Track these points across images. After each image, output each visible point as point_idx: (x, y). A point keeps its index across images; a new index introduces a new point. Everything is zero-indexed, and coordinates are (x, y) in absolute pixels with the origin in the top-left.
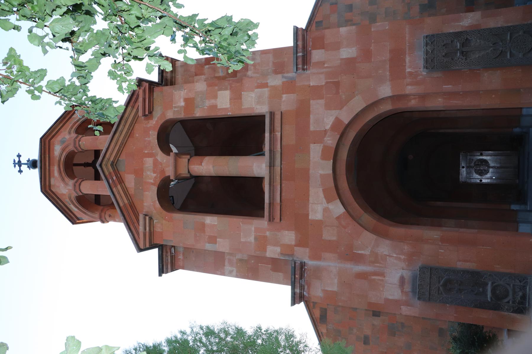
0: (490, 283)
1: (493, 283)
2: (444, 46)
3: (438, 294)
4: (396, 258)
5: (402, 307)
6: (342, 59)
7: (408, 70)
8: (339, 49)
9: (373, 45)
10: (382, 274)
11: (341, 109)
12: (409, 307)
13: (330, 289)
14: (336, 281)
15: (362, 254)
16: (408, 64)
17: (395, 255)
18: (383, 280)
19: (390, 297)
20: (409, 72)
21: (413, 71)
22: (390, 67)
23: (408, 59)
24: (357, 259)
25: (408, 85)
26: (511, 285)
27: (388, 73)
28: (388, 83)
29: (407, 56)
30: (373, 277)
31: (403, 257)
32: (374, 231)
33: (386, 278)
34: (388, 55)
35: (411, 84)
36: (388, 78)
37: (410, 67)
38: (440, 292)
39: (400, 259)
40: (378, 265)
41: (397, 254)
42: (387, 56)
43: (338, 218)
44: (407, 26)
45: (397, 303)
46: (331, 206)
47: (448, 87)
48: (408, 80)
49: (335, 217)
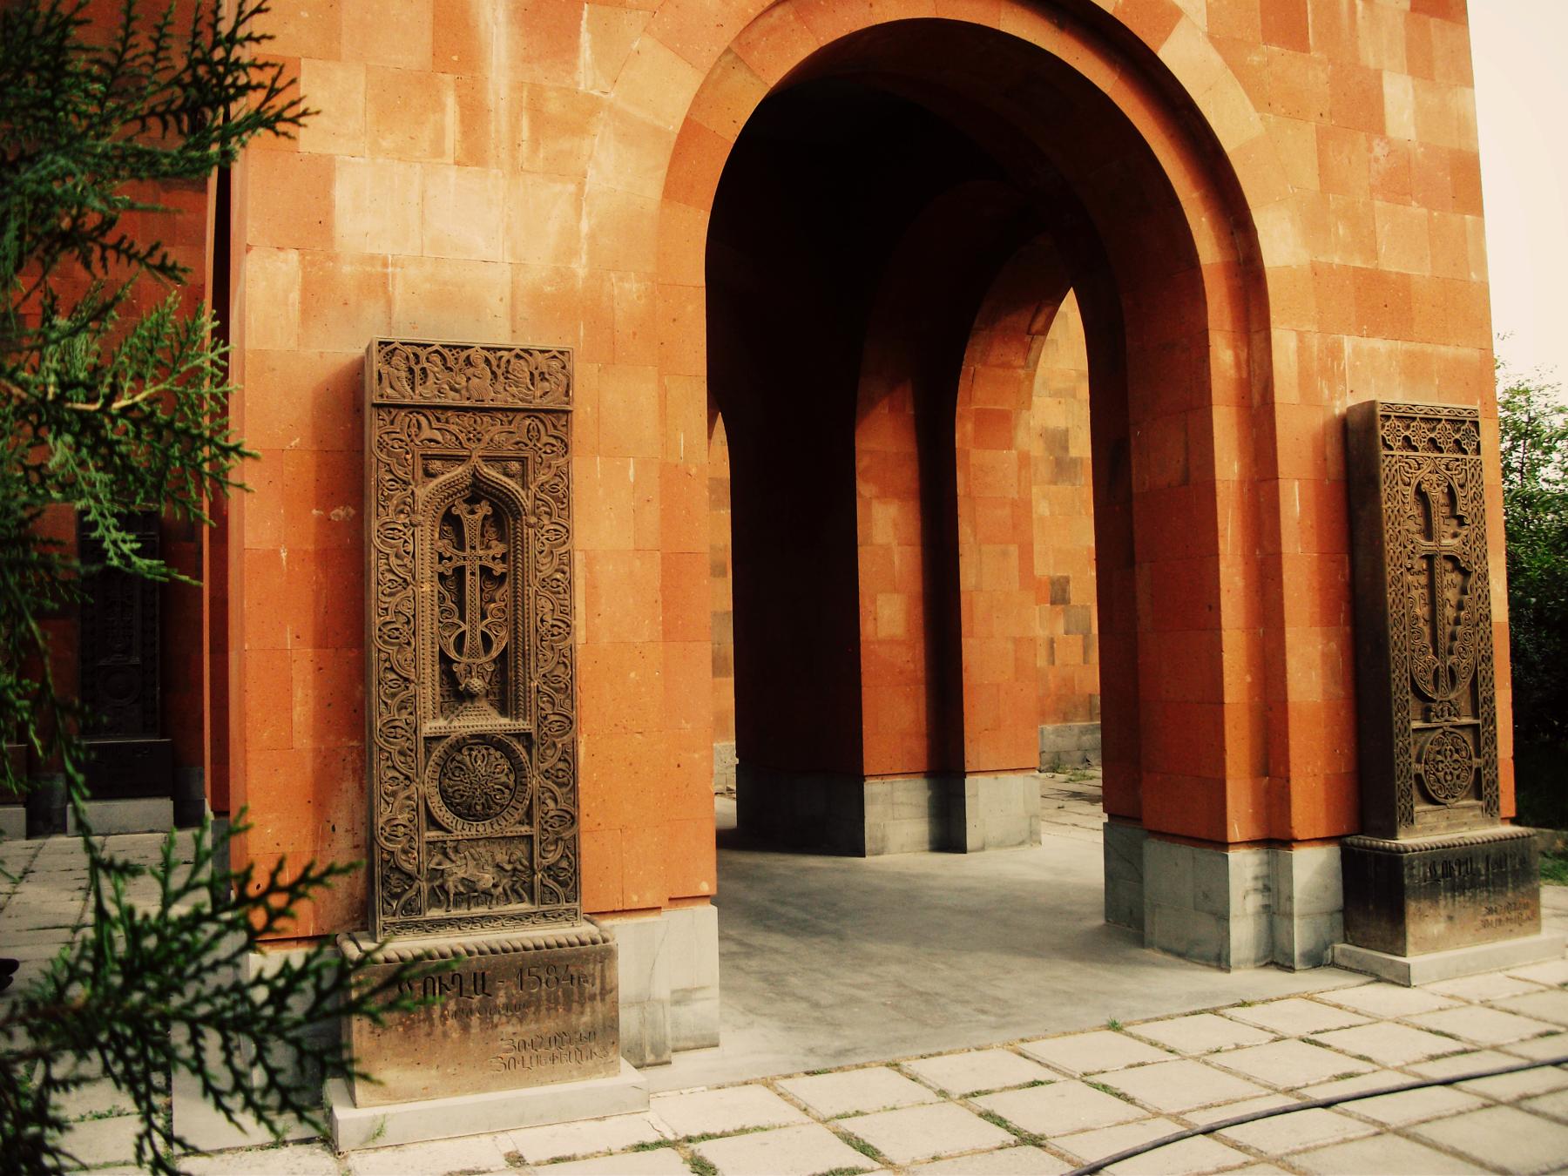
0: (522, 725)
1: (525, 737)
3: (425, 457)
5: (293, 256)
6: (1378, 75)
7: (1348, 343)
8: (1412, 72)
9: (1424, 211)
10: (473, 154)
11: (1211, 37)
12: (295, 296)
15: (574, 49)
17: (585, 227)
18: (438, 150)
19: (342, 193)
20: (1341, 349)
26: (525, 830)
27: (1337, 260)
29: (1390, 344)
30: (450, 102)
31: (580, 267)
32: (691, 130)
33: (453, 173)
34: (1394, 269)
35: (1302, 349)
36: (1322, 259)
37: (1357, 352)
38: (436, 465)
40: (525, 133)
41: (592, 237)
42: (1391, 262)
45: (313, 229)
47: (1296, 501)
48: (1315, 342)
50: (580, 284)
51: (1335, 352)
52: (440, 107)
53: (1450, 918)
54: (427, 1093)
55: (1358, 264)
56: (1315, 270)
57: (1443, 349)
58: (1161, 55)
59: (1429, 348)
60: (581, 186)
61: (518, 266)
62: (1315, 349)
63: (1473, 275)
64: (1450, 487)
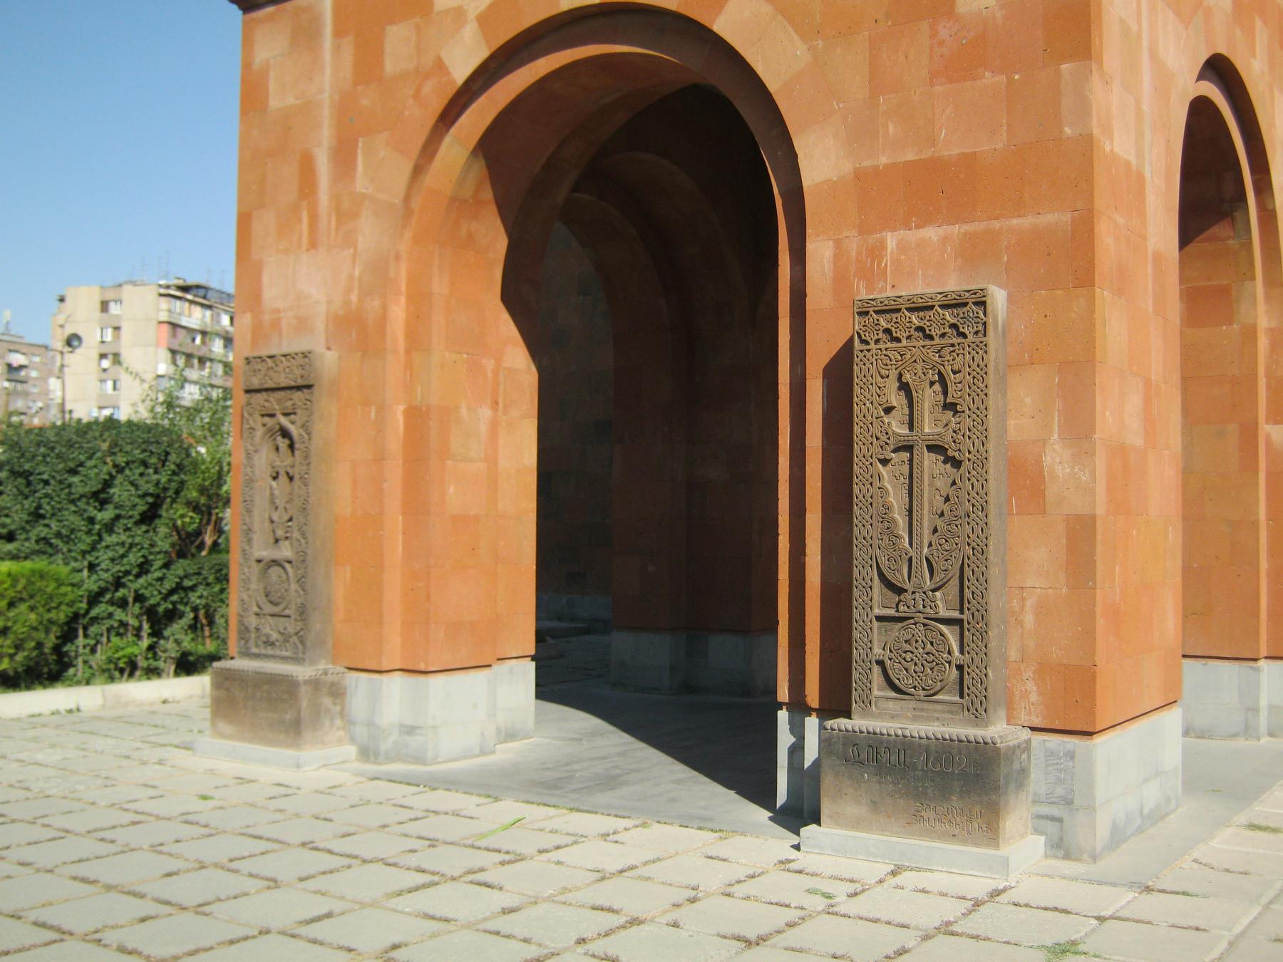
2: (940, 374)
4: (351, 277)
9: (1002, 78)
12: (249, 336)
13: (272, 87)
14: (291, 100)
16: (913, 236)
17: (357, 272)
19: (266, 279)
21: (887, 259)
22: (907, 163)
23: (932, 233)
24: (344, 157)
25: (838, 244)
27: (883, 160)
28: (847, 167)
30: (305, 215)
31: (354, 298)
37: (902, 247)
39: (349, 290)
42: (951, 145)
43: (440, 66)
44: (1067, 217)
46: (470, 31)
49: (443, 55)
50: (354, 307)
51: (877, 251)
52: (300, 220)
53: (874, 803)
54: (231, 737)
55: (910, 157)
56: (859, 175)
57: (1015, 221)
58: (715, 28)
59: (996, 225)
60: (356, 248)
61: (329, 302)
62: (853, 253)
63: (1068, 130)
64: (940, 374)
